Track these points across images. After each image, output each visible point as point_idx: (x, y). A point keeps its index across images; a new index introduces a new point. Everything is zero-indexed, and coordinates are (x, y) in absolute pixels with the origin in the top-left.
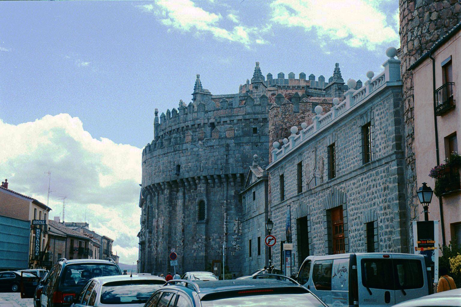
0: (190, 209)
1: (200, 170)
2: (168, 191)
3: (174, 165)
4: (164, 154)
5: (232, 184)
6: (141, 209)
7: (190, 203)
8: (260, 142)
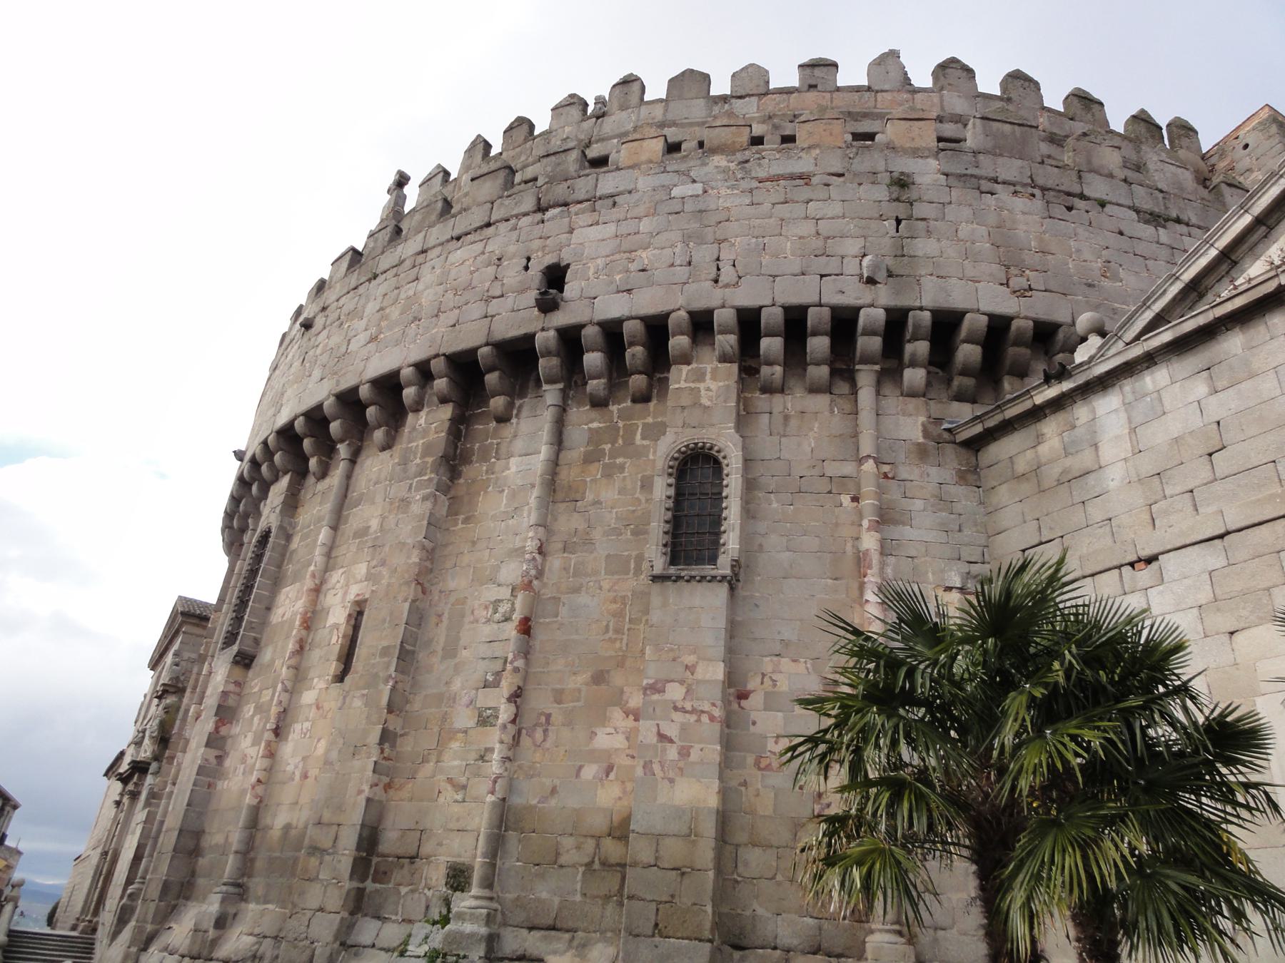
0: (597, 503)
1: (716, 281)
2: (447, 412)
3: (527, 268)
4: (458, 238)
5: (915, 376)
6: (152, 672)
7: (596, 470)
8: (1082, 197)
